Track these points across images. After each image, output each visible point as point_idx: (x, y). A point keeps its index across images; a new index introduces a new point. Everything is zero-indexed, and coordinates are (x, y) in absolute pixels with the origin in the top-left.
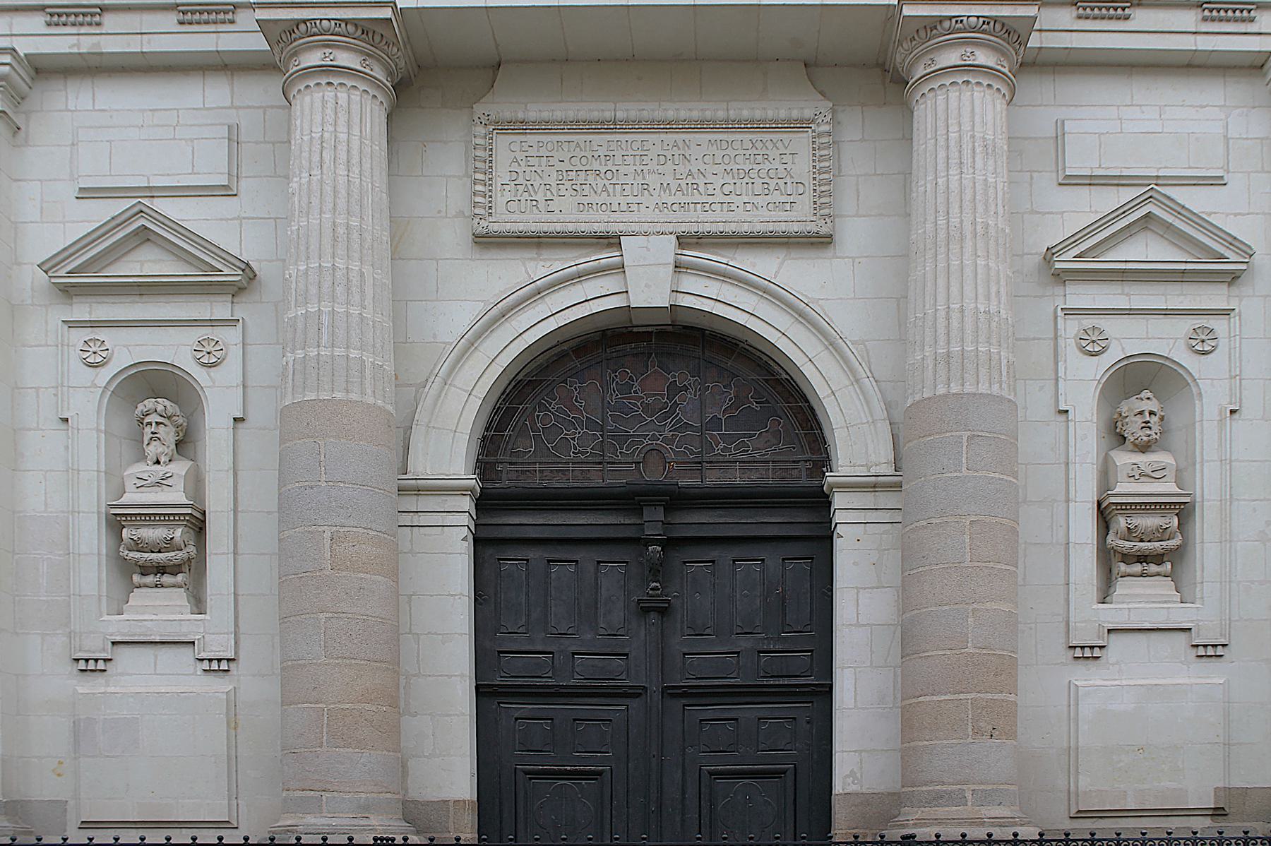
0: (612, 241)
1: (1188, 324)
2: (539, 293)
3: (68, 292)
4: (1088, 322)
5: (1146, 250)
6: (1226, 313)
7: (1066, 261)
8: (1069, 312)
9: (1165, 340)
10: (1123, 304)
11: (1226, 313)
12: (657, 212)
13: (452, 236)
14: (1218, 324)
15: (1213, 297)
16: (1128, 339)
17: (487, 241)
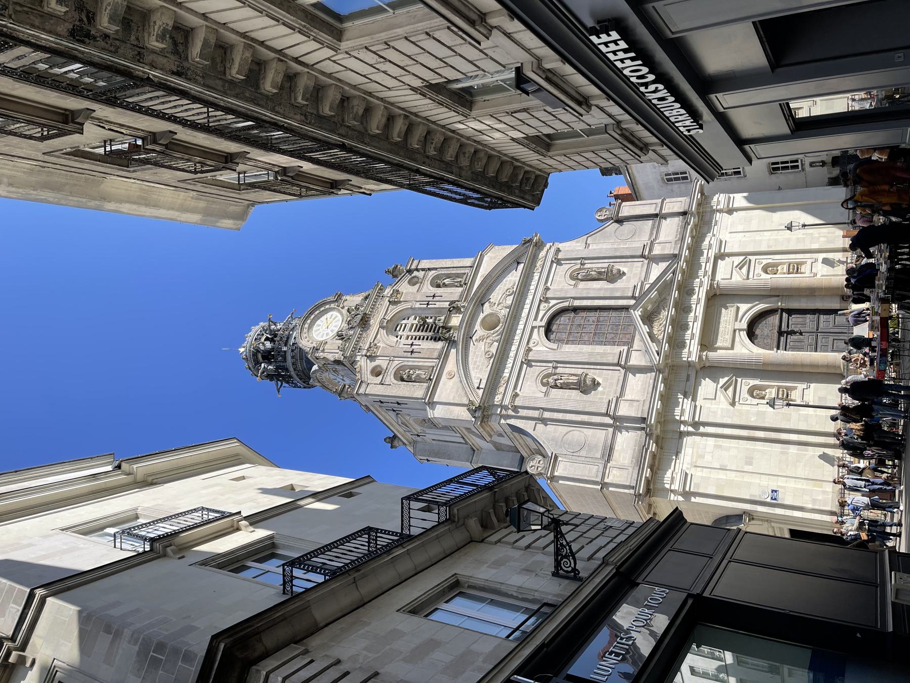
0: (735, 331)
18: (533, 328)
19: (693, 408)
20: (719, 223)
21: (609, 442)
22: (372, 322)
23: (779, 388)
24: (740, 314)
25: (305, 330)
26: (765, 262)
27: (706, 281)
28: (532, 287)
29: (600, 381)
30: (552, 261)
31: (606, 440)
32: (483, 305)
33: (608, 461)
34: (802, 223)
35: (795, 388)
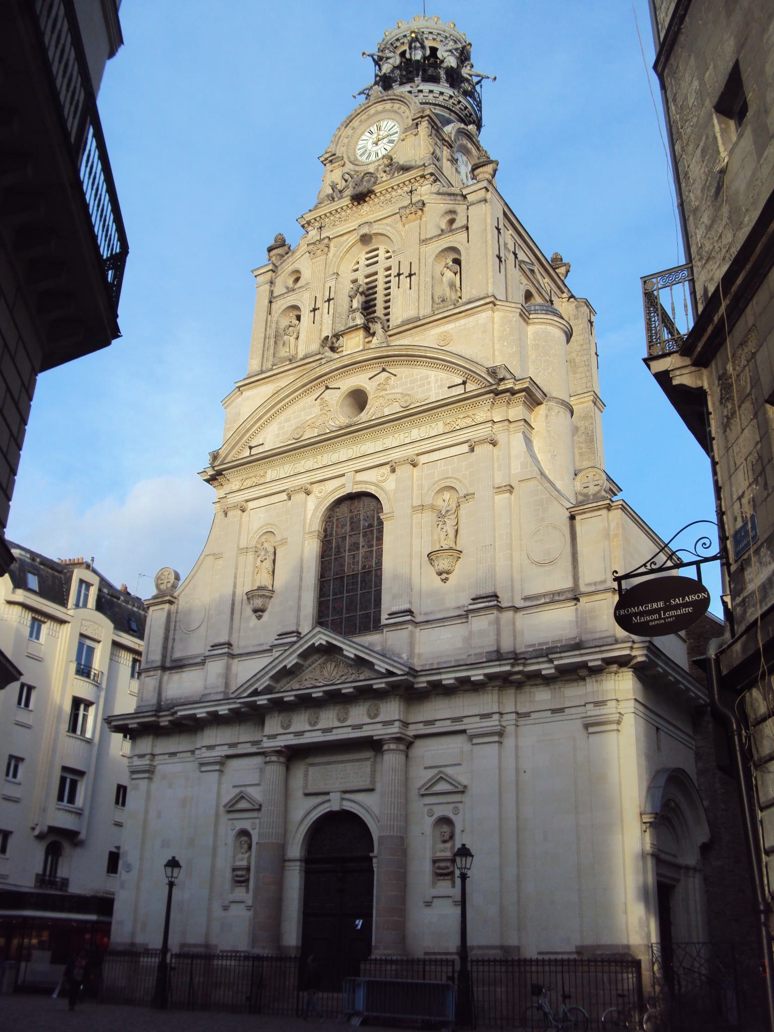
0: (328, 793)
1: (452, 806)
2: (315, 808)
3: (229, 812)
4: (430, 807)
5: (442, 787)
6: (461, 802)
7: (422, 791)
8: (425, 805)
9: (446, 811)
10: (437, 801)
11: (461, 802)
12: (335, 785)
13: (299, 793)
14: (460, 806)
15: (457, 798)
16: (440, 811)
17: (307, 795)
18: (343, 475)
19: (212, 760)
20: (558, 716)
21: (191, 662)
22: (365, 208)
23: (248, 869)
24: (359, 797)
25: (364, 117)
26: (457, 820)
27: (395, 729)
28: (415, 434)
29: (262, 619)
30: (466, 442)
31: (191, 658)
32: (384, 370)
33: (164, 668)
34: (469, 873)
35: (247, 892)
